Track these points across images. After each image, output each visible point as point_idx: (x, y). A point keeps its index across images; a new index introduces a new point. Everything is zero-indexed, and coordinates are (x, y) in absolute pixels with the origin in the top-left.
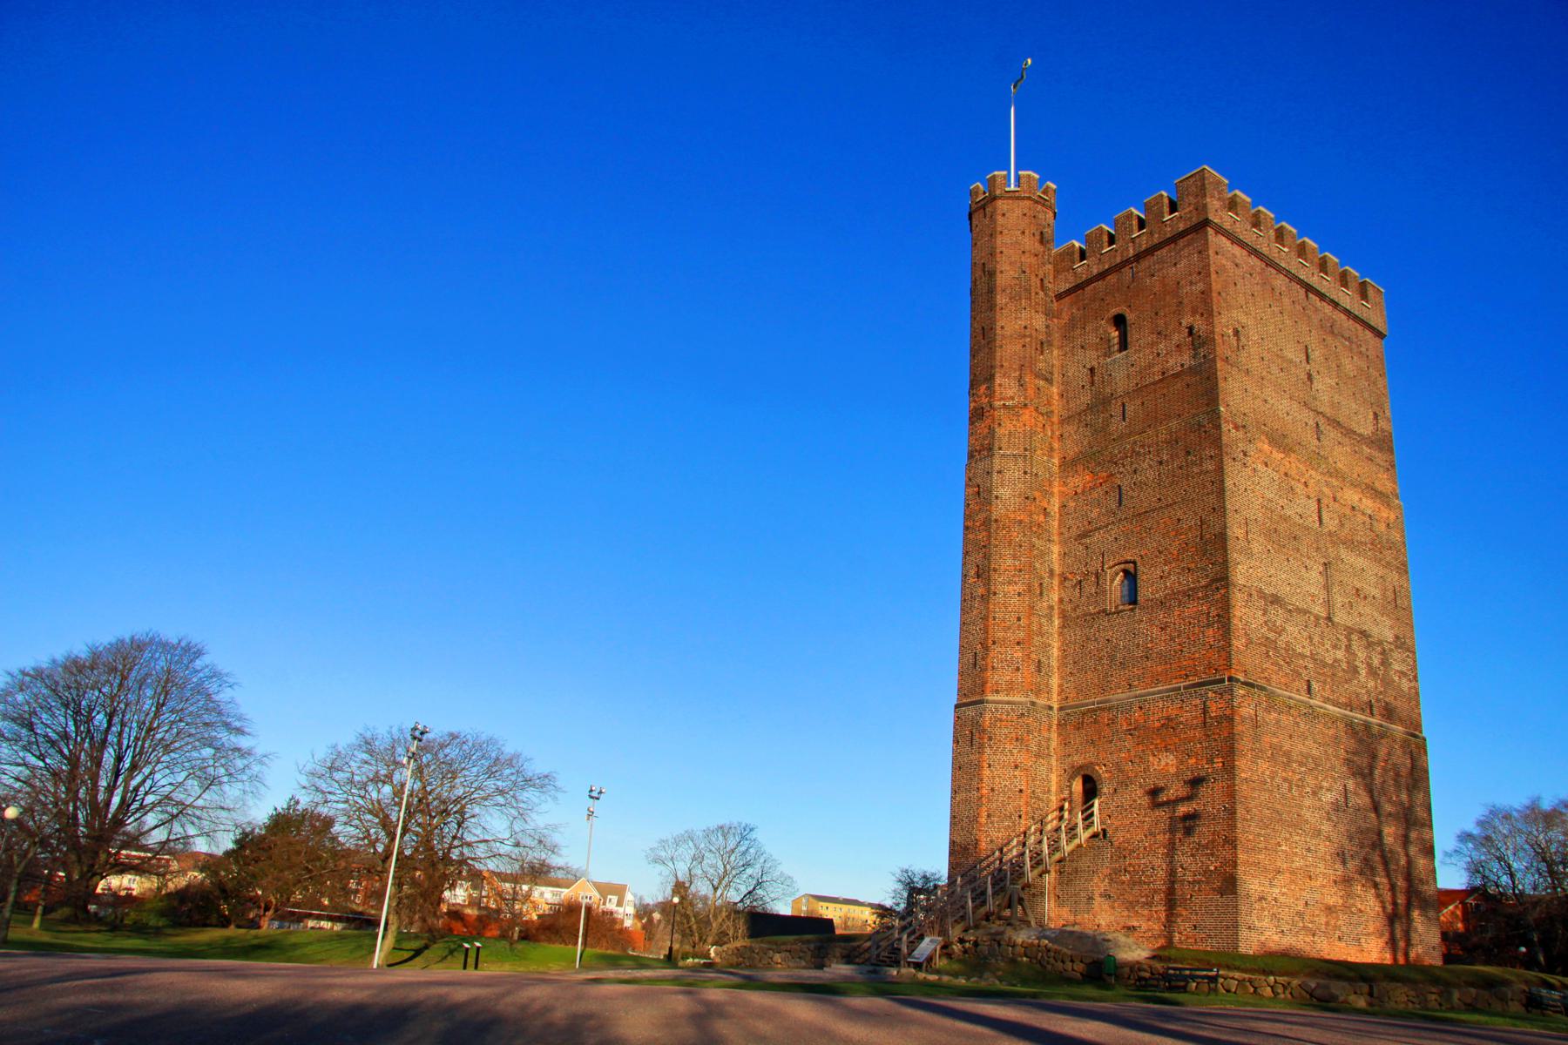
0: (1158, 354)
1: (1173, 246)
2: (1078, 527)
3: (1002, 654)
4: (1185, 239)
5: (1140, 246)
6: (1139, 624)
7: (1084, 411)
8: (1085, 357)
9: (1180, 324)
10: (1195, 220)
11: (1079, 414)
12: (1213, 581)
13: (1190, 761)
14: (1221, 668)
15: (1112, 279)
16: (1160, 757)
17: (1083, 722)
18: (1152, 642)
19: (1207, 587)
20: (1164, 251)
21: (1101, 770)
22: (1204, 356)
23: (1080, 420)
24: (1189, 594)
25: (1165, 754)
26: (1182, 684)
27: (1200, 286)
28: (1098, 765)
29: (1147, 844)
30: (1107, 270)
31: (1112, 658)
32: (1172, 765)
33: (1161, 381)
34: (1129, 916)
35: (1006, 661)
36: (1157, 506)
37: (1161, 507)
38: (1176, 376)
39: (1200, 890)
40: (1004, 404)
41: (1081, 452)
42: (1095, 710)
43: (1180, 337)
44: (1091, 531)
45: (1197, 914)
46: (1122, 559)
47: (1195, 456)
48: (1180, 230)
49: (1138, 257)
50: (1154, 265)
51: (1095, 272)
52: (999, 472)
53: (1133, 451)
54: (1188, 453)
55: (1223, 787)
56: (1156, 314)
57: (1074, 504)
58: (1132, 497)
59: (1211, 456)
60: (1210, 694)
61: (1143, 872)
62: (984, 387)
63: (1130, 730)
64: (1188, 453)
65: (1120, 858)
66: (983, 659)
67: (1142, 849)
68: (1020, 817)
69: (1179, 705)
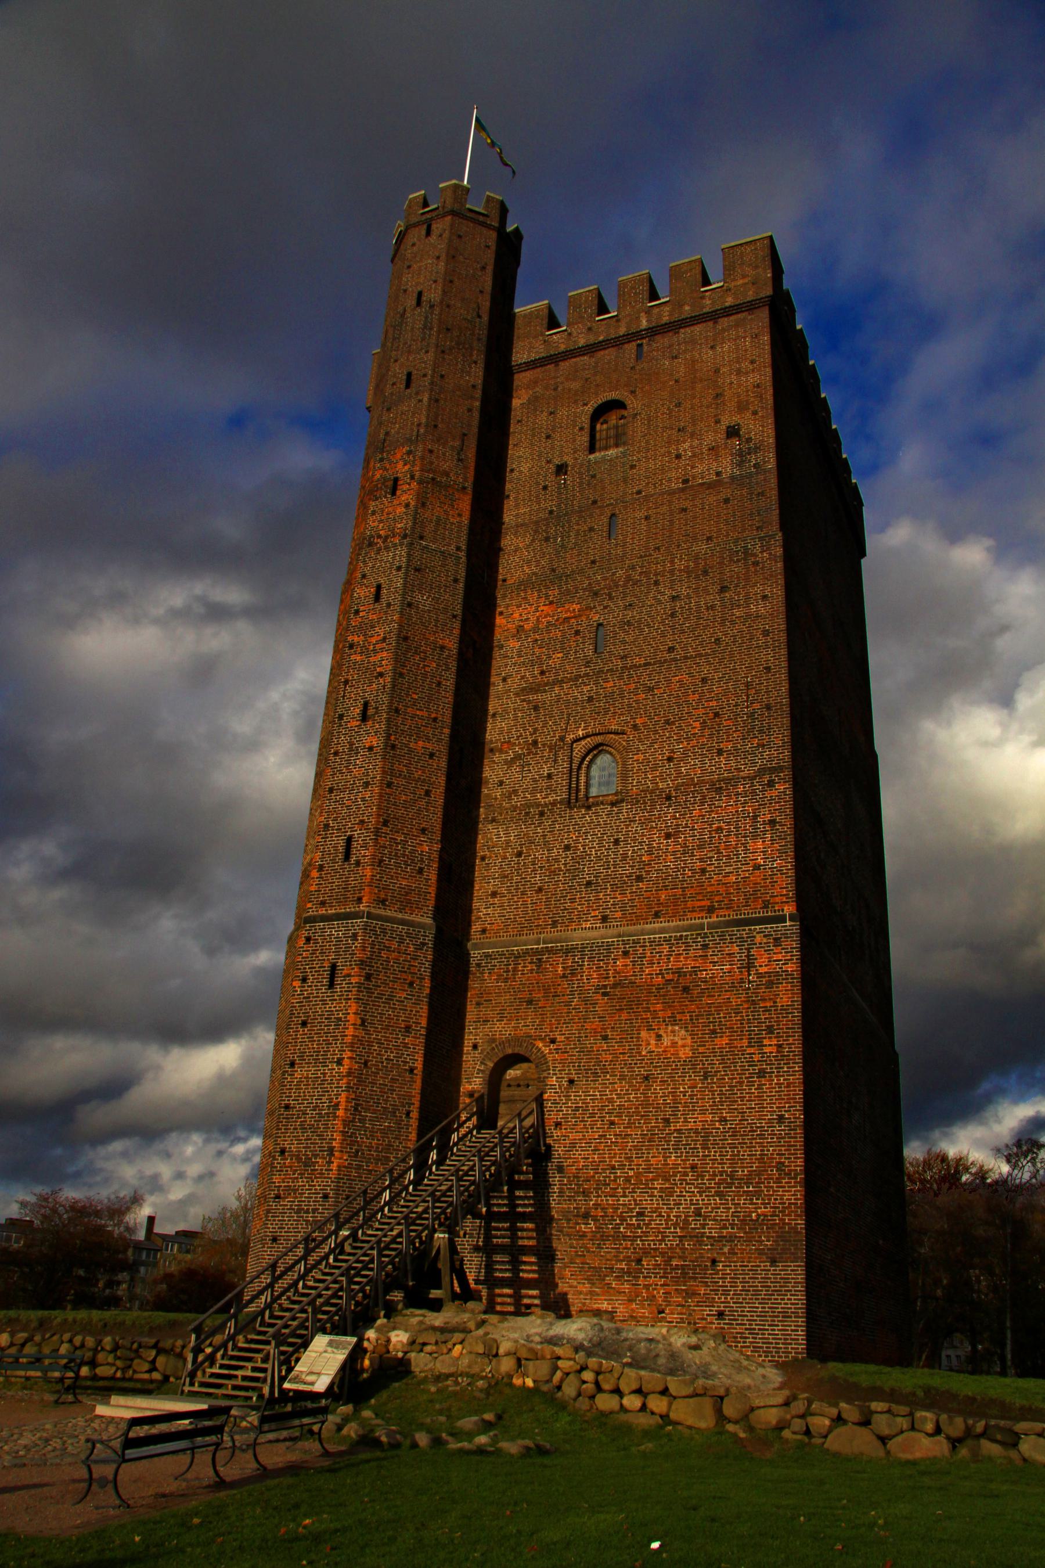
0: (678, 457)
1: (711, 324)
2: (523, 677)
3: (397, 844)
4: (732, 318)
5: (660, 316)
6: (627, 826)
7: (547, 519)
8: (552, 448)
9: (718, 422)
11: (537, 523)
12: (762, 771)
13: (717, 1041)
14: (777, 900)
15: (608, 355)
16: (661, 1032)
17: (515, 970)
18: (650, 852)
20: (697, 328)
23: (536, 531)
25: (670, 1028)
26: (705, 921)
28: (542, 1040)
29: (631, 1173)
30: (600, 342)
31: (573, 873)
32: (683, 1046)
33: (683, 490)
34: (591, 1293)
35: (404, 855)
36: (667, 656)
37: (675, 660)
38: (710, 486)
39: (732, 1252)
40: (433, 479)
41: (534, 574)
42: (537, 952)
43: (713, 436)
44: (546, 684)
45: (726, 1293)
47: (739, 594)
48: (727, 304)
49: (654, 332)
50: (679, 344)
51: (582, 342)
52: (417, 570)
54: (723, 589)
55: (779, 1084)
57: (518, 645)
58: (624, 642)
59: (765, 597)
60: (759, 938)
61: (623, 1219)
63: (605, 987)
64: (723, 589)
65: (577, 1193)
66: (365, 846)
67: (621, 1181)
68: (408, 1114)
69: (701, 953)
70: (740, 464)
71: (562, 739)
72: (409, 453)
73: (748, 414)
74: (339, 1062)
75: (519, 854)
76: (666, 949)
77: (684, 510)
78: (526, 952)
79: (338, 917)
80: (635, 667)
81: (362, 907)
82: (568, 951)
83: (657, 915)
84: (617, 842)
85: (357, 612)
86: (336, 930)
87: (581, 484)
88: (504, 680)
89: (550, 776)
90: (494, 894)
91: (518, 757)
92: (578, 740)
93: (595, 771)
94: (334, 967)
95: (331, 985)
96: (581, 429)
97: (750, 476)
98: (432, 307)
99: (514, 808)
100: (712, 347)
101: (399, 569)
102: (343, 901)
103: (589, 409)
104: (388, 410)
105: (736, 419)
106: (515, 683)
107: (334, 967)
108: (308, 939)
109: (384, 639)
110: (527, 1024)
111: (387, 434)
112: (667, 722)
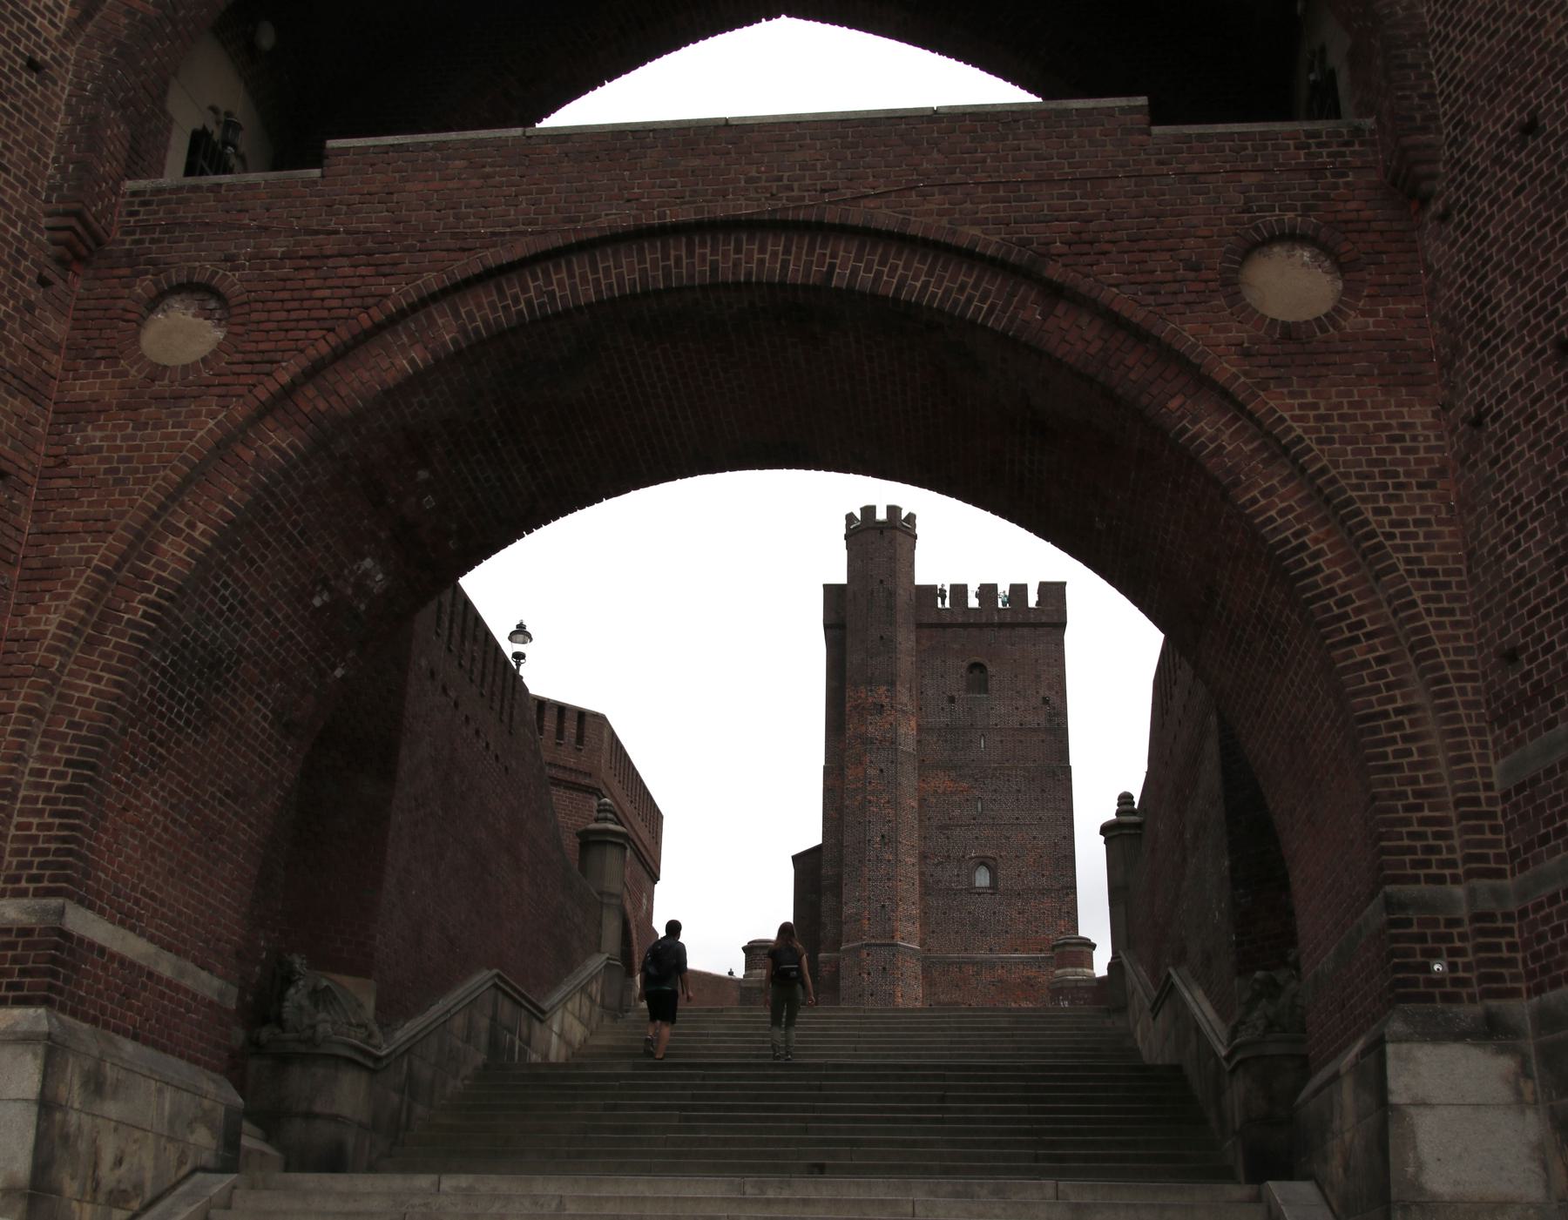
9: (1037, 692)
10: (1055, 619)
12: (1063, 888)
20: (1026, 631)
22: (1058, 724)
30: (971, 624)
38: (1034, 730)
46: (982, 854)
49: (1001, 625)
51: (960, 620)
52: (901, 764)
53: (994, 775)
59: (1063, 799)
62: (885, 688)
66: (893, 911)
71: (963, 857)
72: (888, 690)
73: (1054, 693)
75: (945, 913)
76: (1021, 967)
77: (1021, 741)
78: (953, 963)
79: (883, 945)
82: (974, 963)
83: (1016, 950)
84: (994, 913)
85: (870, 783)
87: (963, 712)
88: (929, 819)
89: (958, 875)
90: (933, 932)
91: (941, 863)
92: (971, 858)
93: (977, 874)
94: (884, 968)
96: (962, 676)
99: (940, 890)
100: (1034, 645)
105: (1047, 693)
107: (884, 968)
108: (868, 955)
109: (888, 802)
111: (873, 674)
112: (1017, 856)
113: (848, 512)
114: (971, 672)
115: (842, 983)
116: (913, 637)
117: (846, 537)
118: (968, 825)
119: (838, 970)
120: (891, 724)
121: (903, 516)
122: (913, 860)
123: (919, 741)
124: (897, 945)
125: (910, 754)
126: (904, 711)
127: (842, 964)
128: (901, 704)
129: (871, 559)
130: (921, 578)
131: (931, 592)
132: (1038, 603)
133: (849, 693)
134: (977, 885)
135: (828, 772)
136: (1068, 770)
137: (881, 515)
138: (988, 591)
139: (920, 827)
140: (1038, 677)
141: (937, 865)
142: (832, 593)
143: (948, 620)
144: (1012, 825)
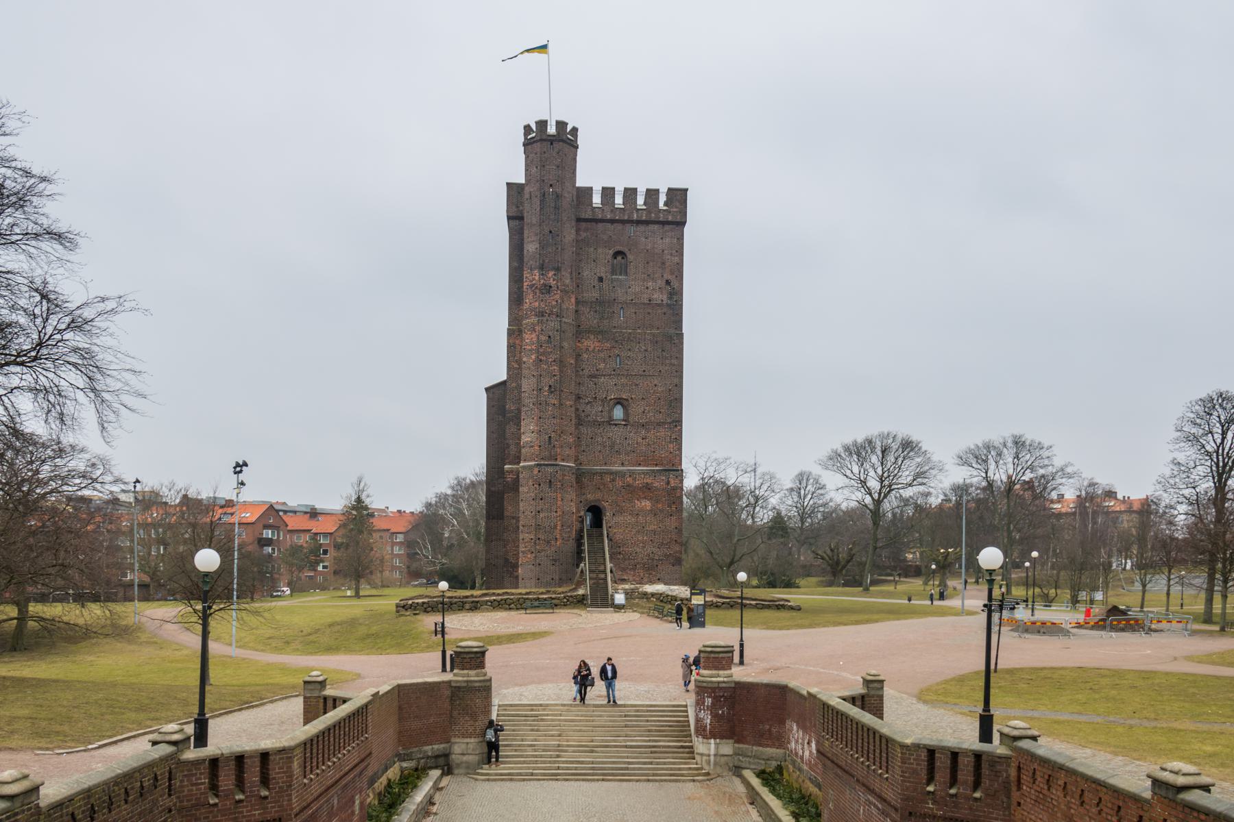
4: (671, 226)
5: (642, 216)
9: (662, 276)
10: (678, 219)
11: (591, 302)
12: (673, 421)
15: (619, 227)
18: (637, 443)
19: (670, 423)
20: (656, 227)
21: (606, 504)
24: (659, 424)
27: (676, 259)
31: (612, 447)
38: (658, 305)
43: (661, 283)
46: (619, 397)
49: (639, 222)
51: (609, 217)
56: (648, 263)
62: (553, 273)
70: (670, 298)
71: (606, 398)
72: (555, 275)
74: (556, 512)
75: (592, 438)
78: (596, 473)
80: (632, 375)
81: (557, 463)
82: (611, 473)
83: (640, 464)
85: (541, 346)
86: (550, 470)
89: (602, 411)
91: (589, 402)
92: (611, 399)
94: (550, 481)
95: (550, 487)
97: (673, 305)
98: (557, 196)
100: (662, 238)
101: (557, 331)
102: (550, 459)
103: (611, 252)
104: (543, 248)
105: (670, 277)
106: (586, 372)
107: (550, 481)
109: (554, 361)
110: (599, 495)
111: (543, 261)
113: (526, 124)
114: (615, 258)
115: (521, 489)
116: (573, 231)
117: (524, 145)
118: (610, 375)
119: (518, 476)
120: (557, 301)
121: (568, 130)
122: (572, 403)
123: (576, 311)
124: (559, 465)
125: (570, 324)
126: (565, 291)
127: (521, 476)
128: (564, 285)
129: (544, 166)
130: (581, 182)
131: (588, 191)
132: (666, 204)
133: (526, 274)
134: (615, 418)
135: (510, 333)
136: (681, 336)
137: (552, 130)
138: (630, 193)
139: (576, 376)
140: (663, 263)
141: (587, 404)
142: (514, 190)
143: (600, 216)
144: (641, 376)
